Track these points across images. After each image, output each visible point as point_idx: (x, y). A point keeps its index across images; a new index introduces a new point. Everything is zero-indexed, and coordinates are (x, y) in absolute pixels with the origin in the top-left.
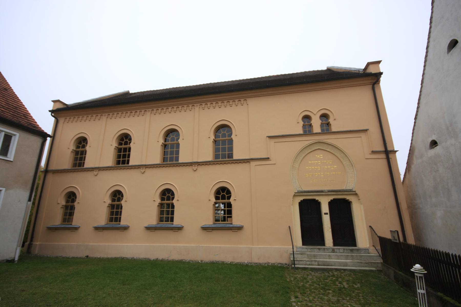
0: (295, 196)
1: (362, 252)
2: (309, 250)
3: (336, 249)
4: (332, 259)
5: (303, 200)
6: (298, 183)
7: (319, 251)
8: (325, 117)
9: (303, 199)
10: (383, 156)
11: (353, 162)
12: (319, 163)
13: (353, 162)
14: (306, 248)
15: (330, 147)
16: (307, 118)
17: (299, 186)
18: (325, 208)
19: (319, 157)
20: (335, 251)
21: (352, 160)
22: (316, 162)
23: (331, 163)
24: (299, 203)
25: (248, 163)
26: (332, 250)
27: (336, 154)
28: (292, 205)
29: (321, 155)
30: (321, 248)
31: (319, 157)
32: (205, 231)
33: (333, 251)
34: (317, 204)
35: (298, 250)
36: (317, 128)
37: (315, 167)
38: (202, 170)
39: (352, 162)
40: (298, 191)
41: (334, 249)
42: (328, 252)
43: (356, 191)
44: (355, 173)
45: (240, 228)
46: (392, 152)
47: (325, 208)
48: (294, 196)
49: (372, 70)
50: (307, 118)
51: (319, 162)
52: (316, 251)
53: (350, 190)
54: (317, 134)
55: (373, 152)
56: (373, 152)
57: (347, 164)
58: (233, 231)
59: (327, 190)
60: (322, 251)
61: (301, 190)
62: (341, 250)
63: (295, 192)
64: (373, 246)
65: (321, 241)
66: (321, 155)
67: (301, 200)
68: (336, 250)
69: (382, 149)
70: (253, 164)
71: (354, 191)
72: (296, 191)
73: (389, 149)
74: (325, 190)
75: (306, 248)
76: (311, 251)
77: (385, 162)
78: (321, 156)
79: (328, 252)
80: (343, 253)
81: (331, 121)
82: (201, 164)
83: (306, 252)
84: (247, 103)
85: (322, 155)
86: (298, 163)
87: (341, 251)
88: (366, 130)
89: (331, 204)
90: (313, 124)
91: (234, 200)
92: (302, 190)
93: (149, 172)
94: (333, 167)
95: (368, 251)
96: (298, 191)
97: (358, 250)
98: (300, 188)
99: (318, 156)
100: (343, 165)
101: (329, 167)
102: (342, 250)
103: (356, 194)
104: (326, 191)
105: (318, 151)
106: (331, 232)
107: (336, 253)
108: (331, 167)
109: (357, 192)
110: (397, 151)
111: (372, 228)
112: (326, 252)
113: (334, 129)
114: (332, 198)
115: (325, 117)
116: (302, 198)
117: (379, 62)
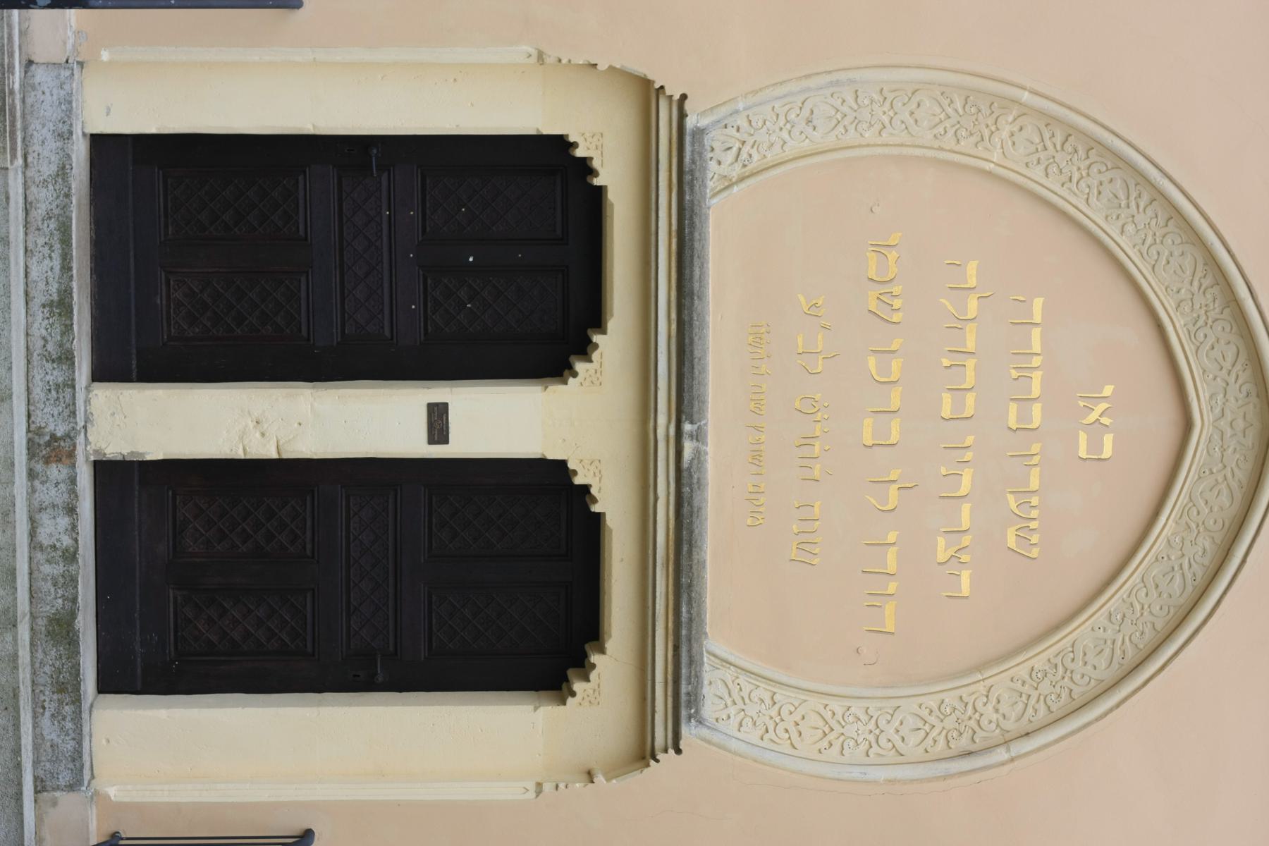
1: (46, 721)
2: (45, 198)
3: (73, 481)
5: (600, 191)
6: (796, 145)
7: (39, 299)
9: (612, 196)
11: (1003, 764)
12: (1013, 407)
13: (1003, 764)
14: (63, 172)
15: (1203, 548)
19: (1093, 417)
20: (47, 461)
22: (1037, 376)
23: (1012, 542)
24: (561, 144)
26: (54, 437)
27: (1113, 600)
28: (541, 56)
29: (1108, 440)
30: (68, 328)
31: (1093, 417)
35: (40, 75)
37: (971, 363)
39: (1001, 755)
40: (699, 133)
41: (71, 454)
42: (38, 392)
43: (678, 751)
44: (881, 774)
48: (646, 83)
51: (1024, 416)
52: (34, 274)
53: (695, 699)
57: (990, 707)
59: (698, 455)
60: (39, 329)
62: (64, 522)
63: (688, 106)
66: (1108, 440)
67: (596, 164)
68: (56, 472)
71: (684, 730)
72: (703, 123)
74: (698, 436)
75: (63, 172)
76: (38, 213)
78: (1095, 445)
79: (38, 392)
80: (34, 545)
83: (20, 161)
85: (1107, 452)
87: (53, 528)
92: (710, 184)
94: (965, 558)
95: (65, 778)
96: (699, 133)
98: (736, 171)
99: (1103, 406)
100: (980, 667)
101: (966, 508)
102: (67, 541)
103: (644, 754)
104: (688, 447)
106: (242, 457)
107: (32, 475)
108: (966, 540)
109: (668, 759)
112: (38, 375)
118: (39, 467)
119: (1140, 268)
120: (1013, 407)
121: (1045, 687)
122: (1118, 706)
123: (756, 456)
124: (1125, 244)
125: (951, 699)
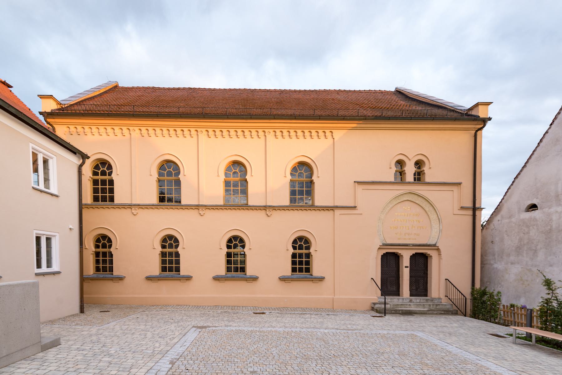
0: (379, 248)
1: (435, 302)
6: (382, 235)
8: (419, 164)
9: (386, 252)
10: (470, 212)
15: (420, 198)
16: (400, 163)
17: (383, 239)
18: (406, 262)
24: (382, 256)
25: (332, 212)
26: (410, 300)
27: (424, 206)
29: (409, 207)
32: (283, 282)
33: (411, 301)
36: (410, 177)
38: (277, 215)
39: (439, 217)
40: (383, 244)
45: (321, 279)
46: (479, 210)
47: (406, 262)
49: (481, 113)
50: (400, 163)
54: (409, 183)
55: (462, 208)
56: (462, 208)
58: (313, 283)
59: (411, 244)
61: (385, 243)
64: (446, 296)
66: (409, 207)
68: (413, 300)
69: (470, 205)
70: (337, 212)
72: (382, 244)
73: (477, 206)
76: (391, 301)
77: (470, 219)
79: (406, 301)
81: (426, 169)
82: (276, 208)
84: (333, 136)
88: (460, 184)
89: (414, 258)
90: (406, 172)
91: (315, 250)
92: (386, 243)
93: (209, 214)
97: (432, 300)
103: (438, 249)
104: (411, 245)
105: (407, 203)
107: (413, 302)
109: (439, 247)
110: (484, 208)
111: (448, 280)
113: (427, 180)
114: (414, 252)
116: (385, 251)
117: (489, 104)
118: (412, 302)
119: (393, 205)
122: (435, 206)
123: (410, 239)
124: (391, 206)
125: (433, 222)
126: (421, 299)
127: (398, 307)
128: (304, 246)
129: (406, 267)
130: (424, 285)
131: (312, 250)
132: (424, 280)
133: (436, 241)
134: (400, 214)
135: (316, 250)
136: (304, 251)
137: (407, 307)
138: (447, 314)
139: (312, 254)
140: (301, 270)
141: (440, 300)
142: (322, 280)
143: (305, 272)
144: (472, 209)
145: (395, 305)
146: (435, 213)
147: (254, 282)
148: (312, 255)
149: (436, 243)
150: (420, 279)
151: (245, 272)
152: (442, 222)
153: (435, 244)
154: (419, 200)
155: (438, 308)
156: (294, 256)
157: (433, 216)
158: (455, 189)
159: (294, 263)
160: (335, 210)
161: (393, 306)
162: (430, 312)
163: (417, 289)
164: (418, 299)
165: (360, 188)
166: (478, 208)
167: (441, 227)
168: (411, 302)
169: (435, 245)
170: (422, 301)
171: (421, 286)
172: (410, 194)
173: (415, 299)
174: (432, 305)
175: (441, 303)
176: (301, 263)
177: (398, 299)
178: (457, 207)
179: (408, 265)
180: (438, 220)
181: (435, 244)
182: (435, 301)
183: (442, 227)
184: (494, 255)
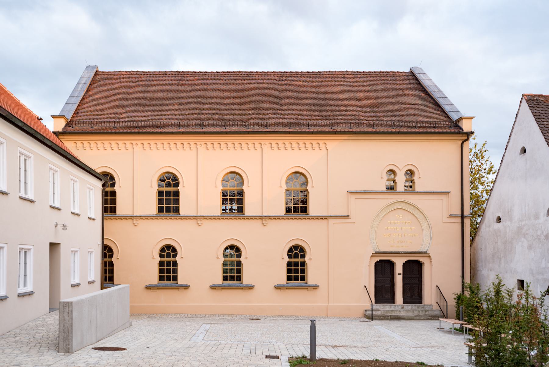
0: (372, 256)
1: (427, 308)
3: (405, 306)
4: (401, 314)
6: (375, 243)
8: (410, 173)
10: (459, 220)
12: (398, 224)
15: (411, 207)
17: (376, 247)
18: (399, 269)
21: (430, 223)
23: (410, 224)
24: (375, 263)
25: (326, 220)
26: (402, 307)
27: (415, 214)
29: (401, 215)
32: (279, 291)
33: (402, 308)
34: (391, 264)
36: (400, 187)
38: (272, 224)
39: (430, 225)
40: (375, 252)
45: (316, 287)
47: (399, 269)
54: (400, 192)
55: (451, 216)
56: (451, 216)
59: (403, 252)
61: (378, 250)
64: (437, 303)
65: (392, 300)
66: (401, 215)
68: (405, 307)
69: (459, 213)
70: (331, 221)
75: (379, 306)
76: (383, 308)
77: (460, 225)
79: (398, 308)
81: (415, 178)
86: (378, 222)
88: (447, 193)
92: (379, 250)
97: (425, 305)
103: (429, 256)
104: (402, 253)
105: (400, 211)
107: (405, 309)
109: (430, 255)
111: (438, 288)
113: (418, 188)
114: (406, 259)
115: (410, 173)
116: (378, 259)
120: (398, 224)
121: (423, 221)
123: (402, 246)
124: (384, 214)
126: (412, 306)
127: (389, 313)
128: (299, 254)
129: (399, 274)
130: (418, 292)
131: (307, 259)
132: (418, 288)
133: (427, 249)
134: (392, 222)
135: (311, 259)
136: (299, 260)
137: (397, 313)
138: (433, 319)
139: (307, 262)
140: (296, 279)
141: (431, 307)
142: (316, 288)
143: (300, 281)
144: (461, 217)
145: (386, 311)
146: (426, 221)
147: (250, 291)
148: (307, 264)
149: (427, 250)
150: (415, 286)
151: (241, 281)
152: (432, 230)
153: (426, 252)
154: (410, 209)
155: (427, 314)
156: (161, 264)
157: (425, 224)
158: (444, 197)
159: (289, 271)
160: (329, 219)
161: (384, 312)
162: (417, 318)
163: (412, 296)
164: (410, 306)
165: (353, 197)
166: (466, 216)
167: (431, 235)
168: (403, 309)
169: (425, 253)
170: (413, 308)
171: (416, 293)
172: (401, 203)
173: (407, 305)
174: (421, 311)
175: (432, 309)
176: (296, 271)
177: (390, 306)
178: (446, 215)
179: (401, 272)
180: (429, 228)
181: (426, 252)
182: (426, 307)
183: (432, 235)
184: (482, 262)
